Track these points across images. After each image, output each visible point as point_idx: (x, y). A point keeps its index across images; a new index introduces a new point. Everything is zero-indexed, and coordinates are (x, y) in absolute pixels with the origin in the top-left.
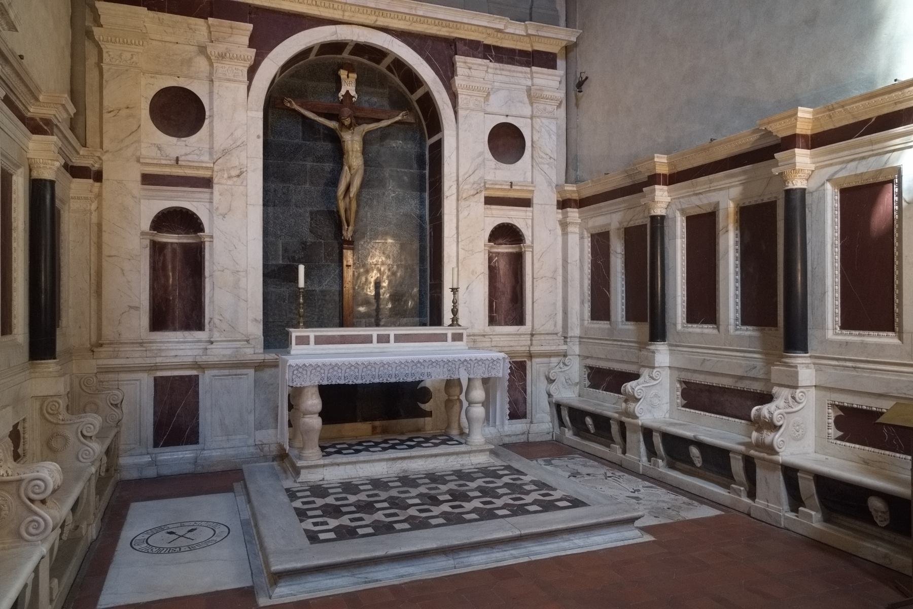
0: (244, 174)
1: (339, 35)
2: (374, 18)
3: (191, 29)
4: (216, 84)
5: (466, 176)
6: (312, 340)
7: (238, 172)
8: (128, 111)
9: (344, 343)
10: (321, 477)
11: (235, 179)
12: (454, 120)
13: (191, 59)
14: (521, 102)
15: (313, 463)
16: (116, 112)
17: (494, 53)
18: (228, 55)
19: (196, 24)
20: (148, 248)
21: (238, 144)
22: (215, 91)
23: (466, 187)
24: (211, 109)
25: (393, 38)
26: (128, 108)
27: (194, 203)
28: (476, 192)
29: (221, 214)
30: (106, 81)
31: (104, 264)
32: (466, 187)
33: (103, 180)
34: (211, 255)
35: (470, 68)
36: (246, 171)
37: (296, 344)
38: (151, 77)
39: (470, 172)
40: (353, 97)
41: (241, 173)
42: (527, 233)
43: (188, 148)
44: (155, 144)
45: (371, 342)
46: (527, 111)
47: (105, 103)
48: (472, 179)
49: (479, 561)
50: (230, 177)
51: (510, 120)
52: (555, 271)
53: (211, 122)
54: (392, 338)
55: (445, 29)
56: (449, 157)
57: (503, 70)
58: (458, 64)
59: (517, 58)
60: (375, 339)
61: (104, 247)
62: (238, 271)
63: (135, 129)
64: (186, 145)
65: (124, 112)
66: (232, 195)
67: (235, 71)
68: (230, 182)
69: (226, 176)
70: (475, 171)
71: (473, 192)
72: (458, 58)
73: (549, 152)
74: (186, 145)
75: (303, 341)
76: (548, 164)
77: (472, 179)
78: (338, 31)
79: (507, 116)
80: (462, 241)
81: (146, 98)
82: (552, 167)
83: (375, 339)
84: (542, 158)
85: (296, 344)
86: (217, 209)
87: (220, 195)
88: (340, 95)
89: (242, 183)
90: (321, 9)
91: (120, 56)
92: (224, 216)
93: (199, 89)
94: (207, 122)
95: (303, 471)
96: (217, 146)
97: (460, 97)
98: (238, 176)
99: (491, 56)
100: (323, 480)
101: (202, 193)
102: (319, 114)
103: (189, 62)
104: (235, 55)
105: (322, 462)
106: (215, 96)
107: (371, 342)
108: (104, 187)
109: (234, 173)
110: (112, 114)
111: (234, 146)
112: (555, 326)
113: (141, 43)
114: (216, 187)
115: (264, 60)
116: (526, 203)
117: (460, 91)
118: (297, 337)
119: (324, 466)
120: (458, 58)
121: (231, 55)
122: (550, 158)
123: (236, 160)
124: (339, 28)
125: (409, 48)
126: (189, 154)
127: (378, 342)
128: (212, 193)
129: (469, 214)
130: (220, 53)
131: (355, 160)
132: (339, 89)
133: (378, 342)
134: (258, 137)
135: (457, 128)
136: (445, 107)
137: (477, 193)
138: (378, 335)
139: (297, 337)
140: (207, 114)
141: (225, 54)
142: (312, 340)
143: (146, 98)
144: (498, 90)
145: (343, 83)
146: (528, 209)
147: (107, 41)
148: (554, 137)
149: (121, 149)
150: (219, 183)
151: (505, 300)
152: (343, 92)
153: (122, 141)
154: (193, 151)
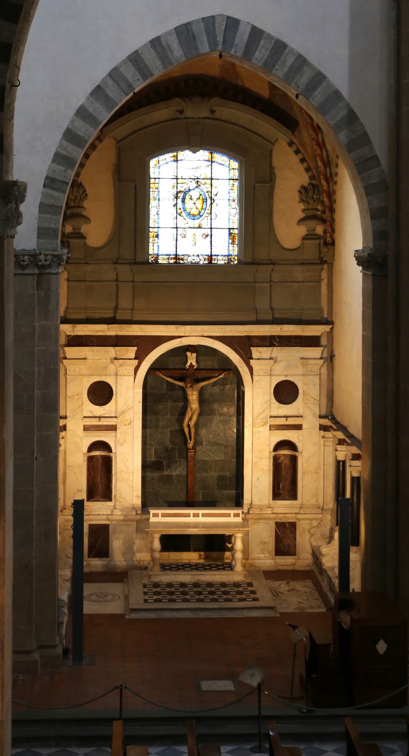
0: (132, 423)
1: (183, 343)
2: (202, 333)
3: (107, 352)
4: (119, 378)
5: (258, 415)
6: (160, 515)
7: (129, 422)
8: (77, 396)
9: (176, 517)
10: (160, 580)
11: (128, 426)
12: (252, 382)
13: (106, 367)
14: (296, 367)
15: (156, 573)
16: (72, 397)
17: (277, 340)
18: (124, 364)
19: (109, 350)
20: (86, 461)
21: (129, 407)
22: (118, 382)
23: (257, 421)
24: (116, 390)
25: (214, 340)
26: (78, 395)
27: (108, 438)
28: (264, 423)
29: (120, 444)
30: (68, 383)
31: (67, 470)
32: (257, 421)
33: (67, 430)
34: (116, 464)
35: (260, 353)
36: (133, 421)
37: (153, 517)
38: (88, 378)
39: (261, 412)
40: (195, 366)
41: (131, 422)
42: (299, 445)
43: (105, 411)
44: (89, 410)
45: (190, 517)
46: (300, 371)
47: (68, 393)
48: (261, 417)
49: (202, 615)
50: (125, 425)
51: (288, 378)
52: (318, 468)
53: (116, 397)
54: (200, 515)
55: (245, 333)
56: (248, 403)
57: (283, 350)
58: (253, 352)
59: (293, 340)
60: (192, 515)
61: (67, 462)
62: (129, 472)
63: (80, 404)
64: (104, 410)
65: (76, 397)
66: (126, 434)
67: (128, 371)
68: (125, 428)
69: (123, 424)
70: (264, 411)
71: (263, 423)
72: (252, 348)
73: (314, 397)
74: (104, 410)
75: (156, 515)
76: (314, 404)
77: (261, 417)
78: (182, 341)
79: (286, 376)
80: (255, 452)
81: (86, 388)
82: (316, 406)
83: (192, 515)
84: (309, 400)
85: (153, 517)
86: (119, 441)
87: (120, 434)
88: (187, 366)
89: (131, 427)
90: (172, 333)
91: (75, 370)
92: (122, 445)
93: (110, 381)
94: (114, 397)
95: (152, 577)
96: (119, 410)
97: (254, 369)
98: (129, 424)
99: (276, 342)
100: (160, 581)
101: (112, 433)
102: (175, 379)
103: (105, 368)
104: (128, 364)
105: (160, 573)
106: (118, 385)
107: (190, 517)
108: (67, 433)
109: (127, 422)
110: (71, 398)
111: (127, 409)
112: (317, 500)
113: (84, 364)
114: (118, 430)
115: (143, 362)
116: (299, 427)
117: (253, 367)
118: (153, 514)
119: (161, 575)
120: (252, 348)
121: (126, 364)
122: (315, 399)
123: (128, 416)
124: (182, 339)
125: (223, 344)
126: (105, 414)
127: (193, 517)
128: (116, 433)
129: (259, 437)
130: (121, 364)
131: (194, 405)
132: (187, 362)
133: (193, 517)
134: (140, 402)
135: (253, 386)
136: (246, 374)
137: (265, 424)
138: (193, 514)
139: (153, 514)
140: (114, 393)
141: (123, 364)
142: (160, 515)
143: (86, 388)
144: (281, 361)
145: (188, 358)
146: (300, 431)
147: (69, 365)
148: (318, 387)
149: (74, 415)
150: (119, 429)
151: (285, 484)
152: (188, 364)
153: (75, 411)
154: (107, 412)
